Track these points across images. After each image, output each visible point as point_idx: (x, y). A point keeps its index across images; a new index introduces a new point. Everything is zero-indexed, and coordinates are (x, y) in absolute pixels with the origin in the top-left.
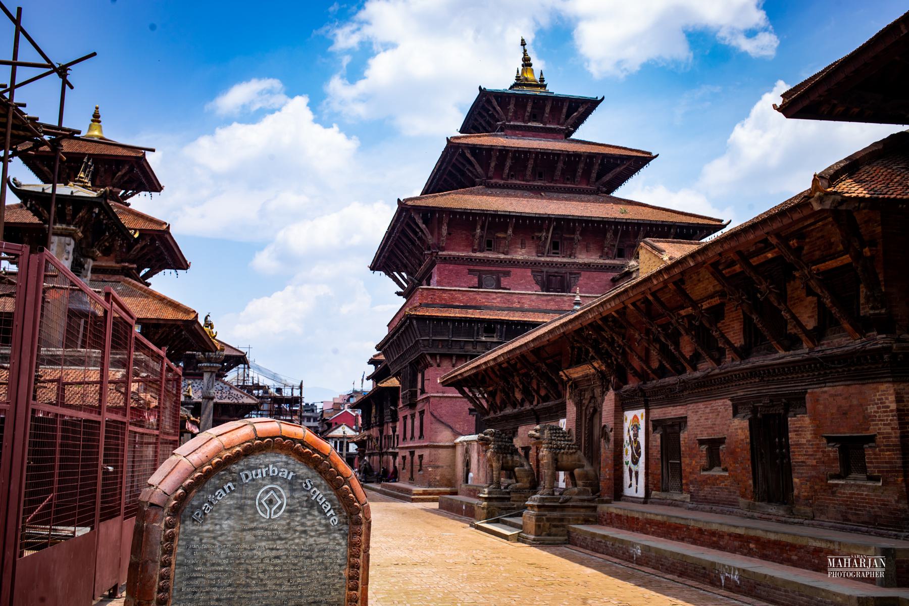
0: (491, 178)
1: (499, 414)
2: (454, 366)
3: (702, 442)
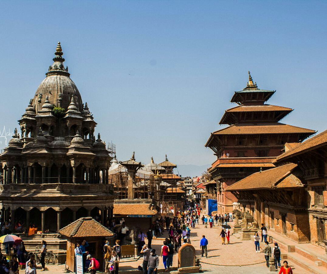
0: (240, 120)
2: (231, 181)
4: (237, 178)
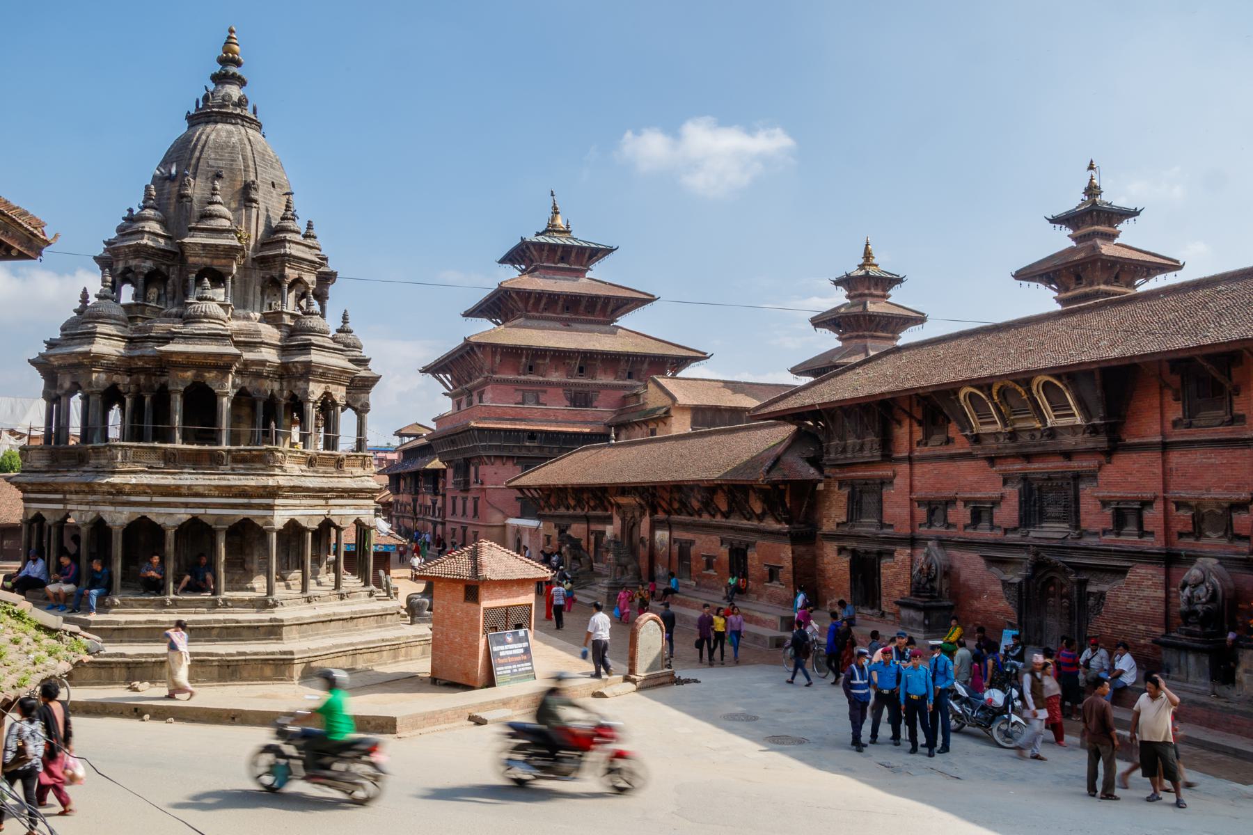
0: (529, 312)
1: (553, 512)
3: (703, 556)
4: (518, 458)
